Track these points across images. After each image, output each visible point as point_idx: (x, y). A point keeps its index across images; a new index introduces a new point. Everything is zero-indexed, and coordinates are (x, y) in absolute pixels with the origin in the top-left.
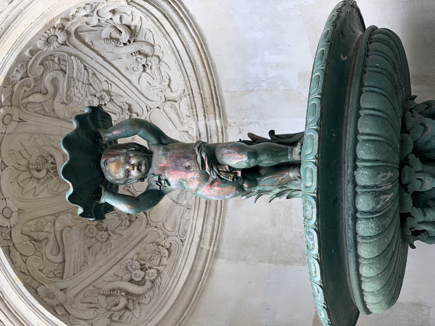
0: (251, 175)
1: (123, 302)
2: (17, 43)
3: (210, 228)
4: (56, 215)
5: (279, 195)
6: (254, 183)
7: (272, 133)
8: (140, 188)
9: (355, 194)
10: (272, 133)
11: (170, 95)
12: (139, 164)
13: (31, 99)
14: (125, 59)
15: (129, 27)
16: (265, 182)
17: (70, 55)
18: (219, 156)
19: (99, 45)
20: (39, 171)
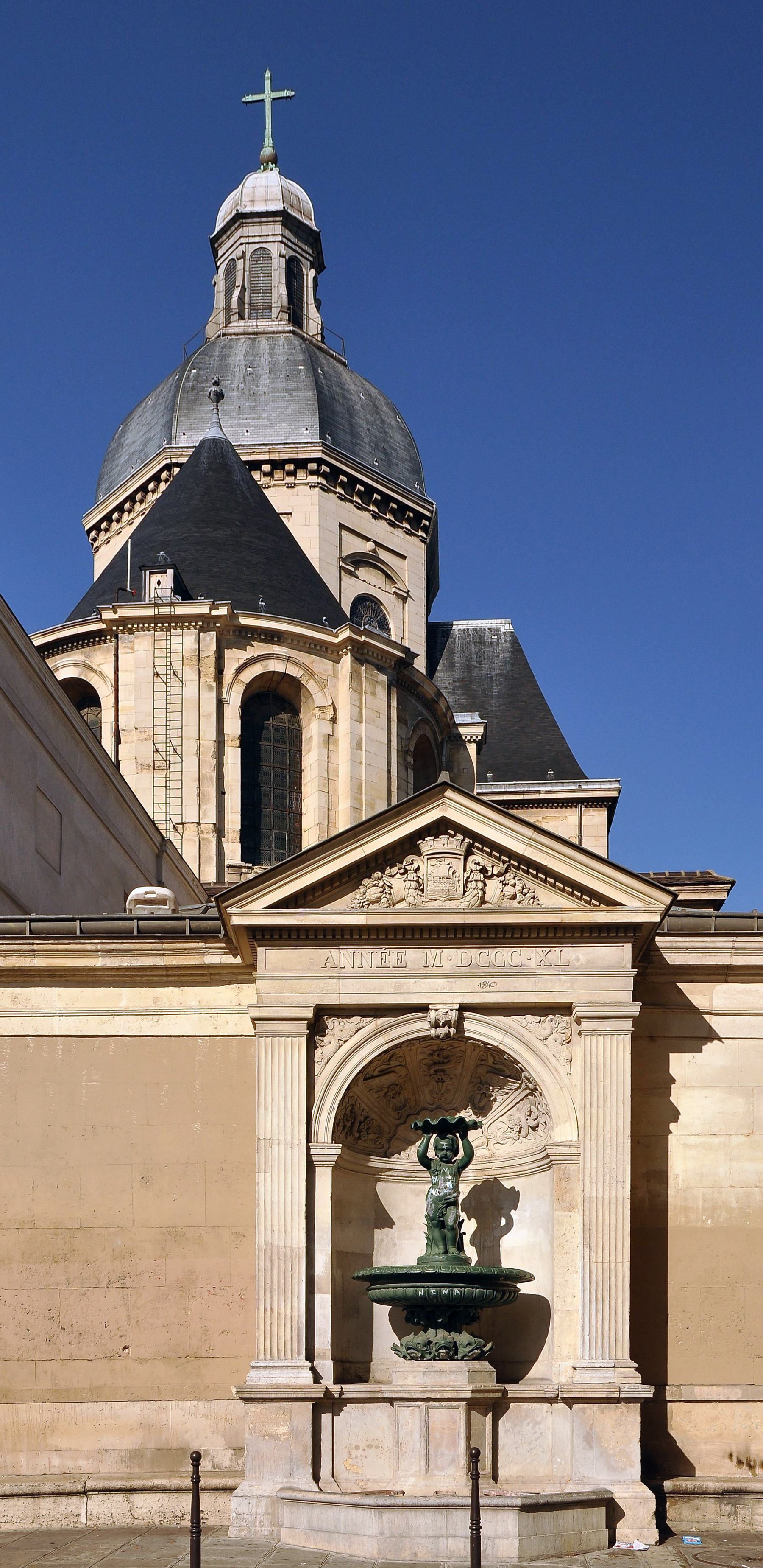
0: (442, 1225)
1: (349, 1124)
2: (526, 1061)
3: (396, 1174)
4: (405, 1066)
5: (428, 1238)
6: (436, 1226)
7: (464, 1233)
8: (431, 1154)
9: (437, 1287)
10: (464, 1233)
11: (491, 1143)
12: (446, 1158)
13: (490, 1057)
14: (518, 1116)
15: (538, 1126)
16: (437, 1233)
17: (521, 1084)
18: (452, 1207)
19: (525, 1106)
20: (438, 1055)
